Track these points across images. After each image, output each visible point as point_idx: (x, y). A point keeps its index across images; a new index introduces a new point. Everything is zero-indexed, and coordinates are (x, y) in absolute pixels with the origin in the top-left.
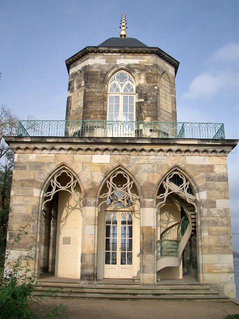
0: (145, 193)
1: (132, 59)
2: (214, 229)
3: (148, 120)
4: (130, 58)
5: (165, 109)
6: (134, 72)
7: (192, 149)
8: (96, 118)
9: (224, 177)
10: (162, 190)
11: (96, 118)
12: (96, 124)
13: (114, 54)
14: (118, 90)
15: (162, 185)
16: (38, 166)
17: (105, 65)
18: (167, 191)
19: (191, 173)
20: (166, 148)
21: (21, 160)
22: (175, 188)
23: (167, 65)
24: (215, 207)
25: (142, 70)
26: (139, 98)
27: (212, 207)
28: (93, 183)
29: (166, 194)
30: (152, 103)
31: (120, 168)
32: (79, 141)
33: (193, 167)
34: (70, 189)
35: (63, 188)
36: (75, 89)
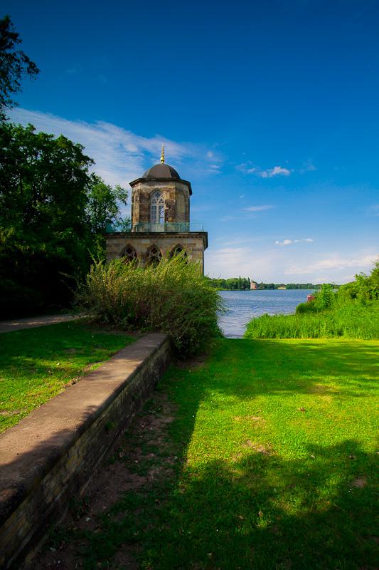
3: (170, 219)
16: (117, 245)
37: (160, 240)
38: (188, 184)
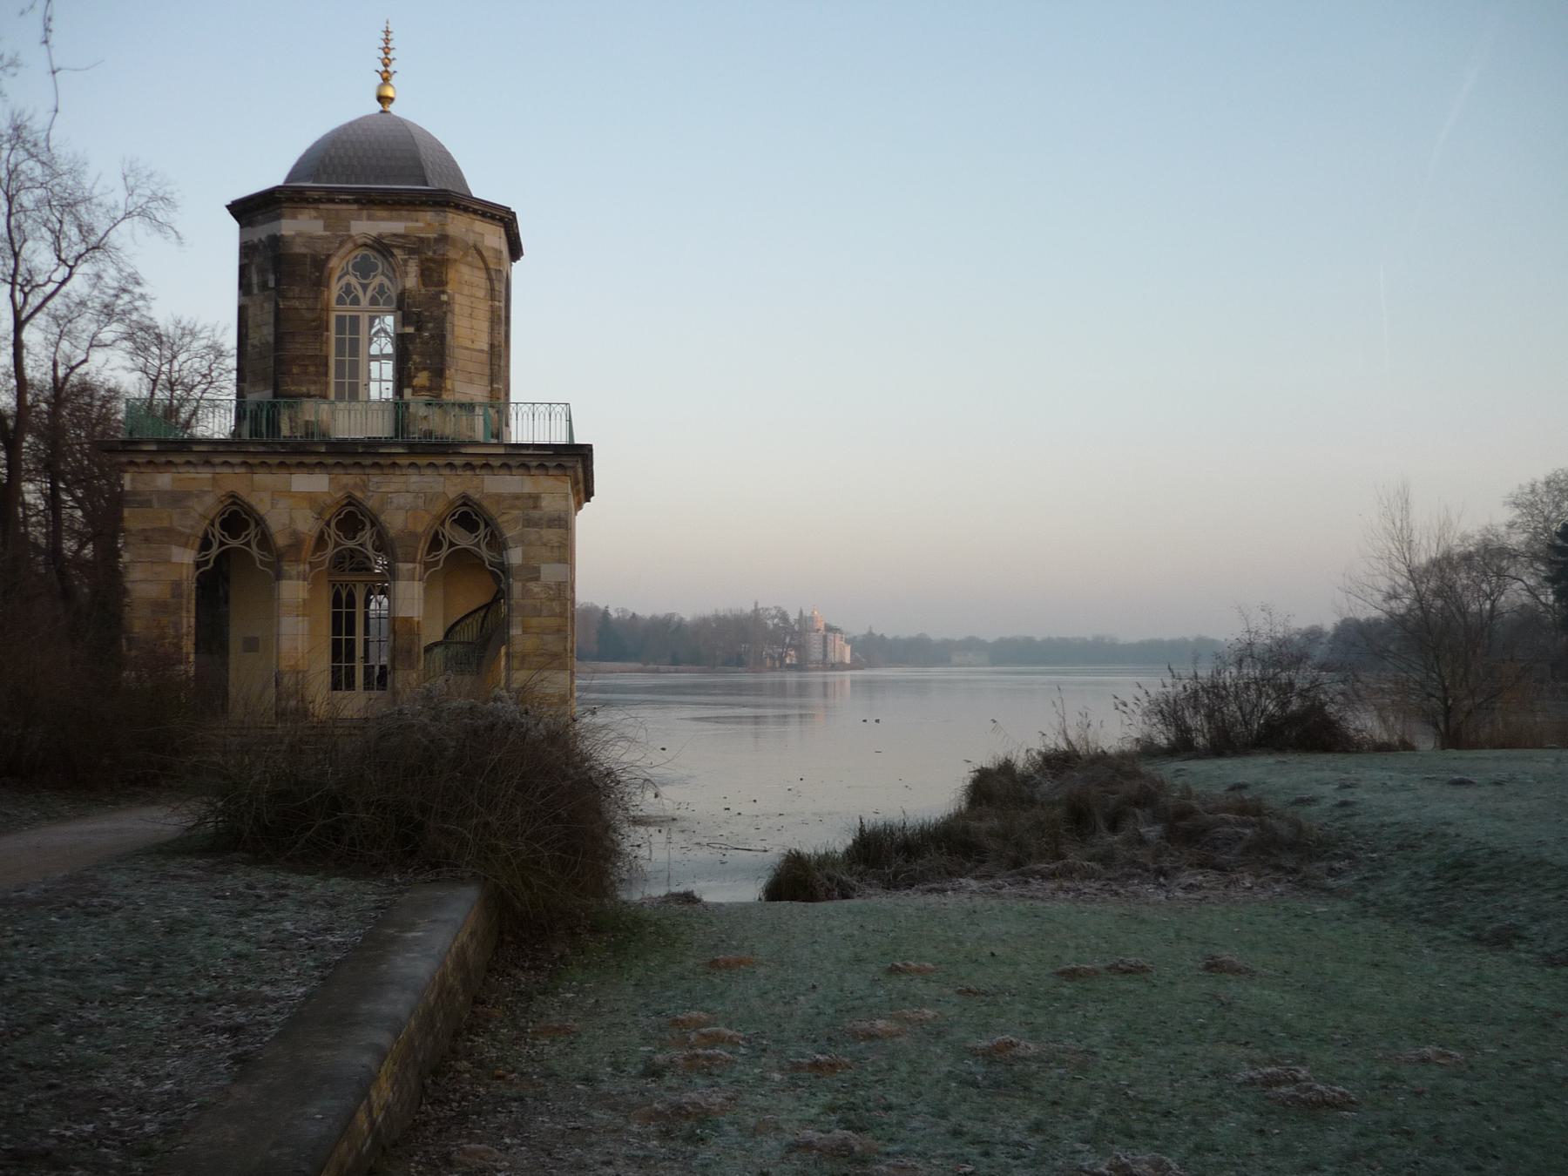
0: (399, 552)
1: (390, 219)
2: (534, 621)
4: (383, 219)
5: (468, 344)
6: (392, 255)
7: (496, 462)
8: (306, 373)
9: (559, 518)
10: (435, 544)
11: (306, 373)
12: (304, 389)
13: (344, 207)
14: (356, 301)
15: (437, 533)
16: (177, 499)
17: (321, 238)
18: (445, 547)
19: (493, 510)
20: (440, 461)
21: (141, 487)
22: (464, 540)
23: (480, 226)
24: (537, 579)
25: (411, 252)
26: (404, 325)
27: (532, 579)
28: (295, 534)
29: (444, 552)
30: (432, 336)
31: (351, 501)
32: (262, 449)
33: (499, 498)
34: (248, 544)
35: (234, 543)
36: (256, 291)
37: (375, 479)
38: (505, 219)
